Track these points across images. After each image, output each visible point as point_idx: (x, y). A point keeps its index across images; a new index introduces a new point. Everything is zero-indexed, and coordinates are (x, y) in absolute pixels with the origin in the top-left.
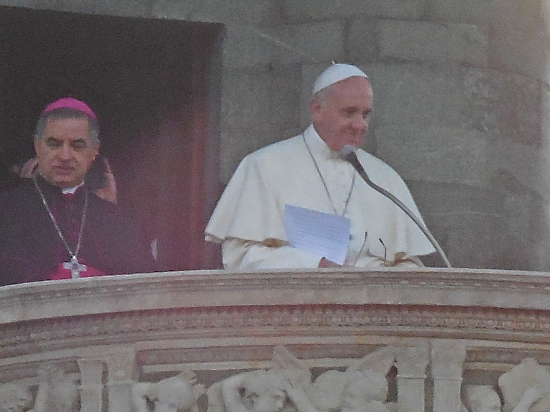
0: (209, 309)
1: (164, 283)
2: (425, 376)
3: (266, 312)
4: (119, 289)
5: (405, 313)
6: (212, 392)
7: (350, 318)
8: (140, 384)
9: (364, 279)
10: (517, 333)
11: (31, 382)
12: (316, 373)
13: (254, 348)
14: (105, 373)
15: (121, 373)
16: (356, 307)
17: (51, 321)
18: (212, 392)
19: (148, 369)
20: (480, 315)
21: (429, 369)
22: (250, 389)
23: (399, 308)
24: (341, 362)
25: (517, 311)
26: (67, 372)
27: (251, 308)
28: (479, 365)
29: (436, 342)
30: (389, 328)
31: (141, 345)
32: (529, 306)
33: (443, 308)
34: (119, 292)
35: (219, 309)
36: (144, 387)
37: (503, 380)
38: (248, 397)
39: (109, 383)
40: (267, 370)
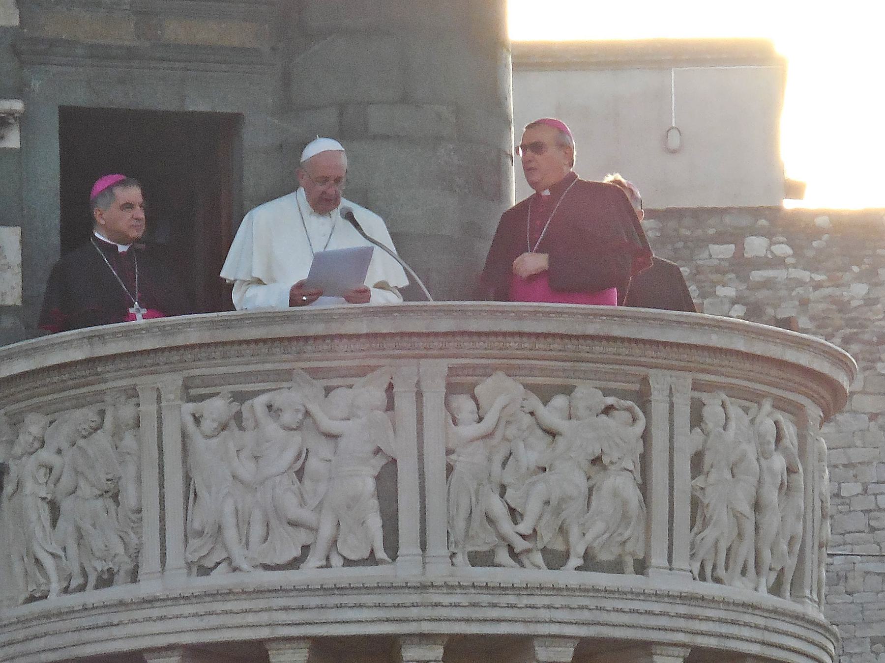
0: (240, 342)
1: (202, 322)
2: (416, 390)
9: (363, 313)
11: (100, 406)
12: (328, 390)
14: (159, 399)
15: (172, 396)
16: (358, 336)
17: (113, 358)
19: (193, 392)
20: (458, 338)
21: (418, 384)
22: (276, 405)
23: (392, 335)
24: (349, 381)
25: (487, 334)
26: (129, 397)
27: (273, 340)
28: (458, 379)
29: (423, 361)
30: (384, 353)
31: (186, 373)
32: (497, 329)
33: (428, 335)
34: (167, 330)
35: (248, 342)
36: (191, 407)
37: (478, 390)
40: (289, 388)
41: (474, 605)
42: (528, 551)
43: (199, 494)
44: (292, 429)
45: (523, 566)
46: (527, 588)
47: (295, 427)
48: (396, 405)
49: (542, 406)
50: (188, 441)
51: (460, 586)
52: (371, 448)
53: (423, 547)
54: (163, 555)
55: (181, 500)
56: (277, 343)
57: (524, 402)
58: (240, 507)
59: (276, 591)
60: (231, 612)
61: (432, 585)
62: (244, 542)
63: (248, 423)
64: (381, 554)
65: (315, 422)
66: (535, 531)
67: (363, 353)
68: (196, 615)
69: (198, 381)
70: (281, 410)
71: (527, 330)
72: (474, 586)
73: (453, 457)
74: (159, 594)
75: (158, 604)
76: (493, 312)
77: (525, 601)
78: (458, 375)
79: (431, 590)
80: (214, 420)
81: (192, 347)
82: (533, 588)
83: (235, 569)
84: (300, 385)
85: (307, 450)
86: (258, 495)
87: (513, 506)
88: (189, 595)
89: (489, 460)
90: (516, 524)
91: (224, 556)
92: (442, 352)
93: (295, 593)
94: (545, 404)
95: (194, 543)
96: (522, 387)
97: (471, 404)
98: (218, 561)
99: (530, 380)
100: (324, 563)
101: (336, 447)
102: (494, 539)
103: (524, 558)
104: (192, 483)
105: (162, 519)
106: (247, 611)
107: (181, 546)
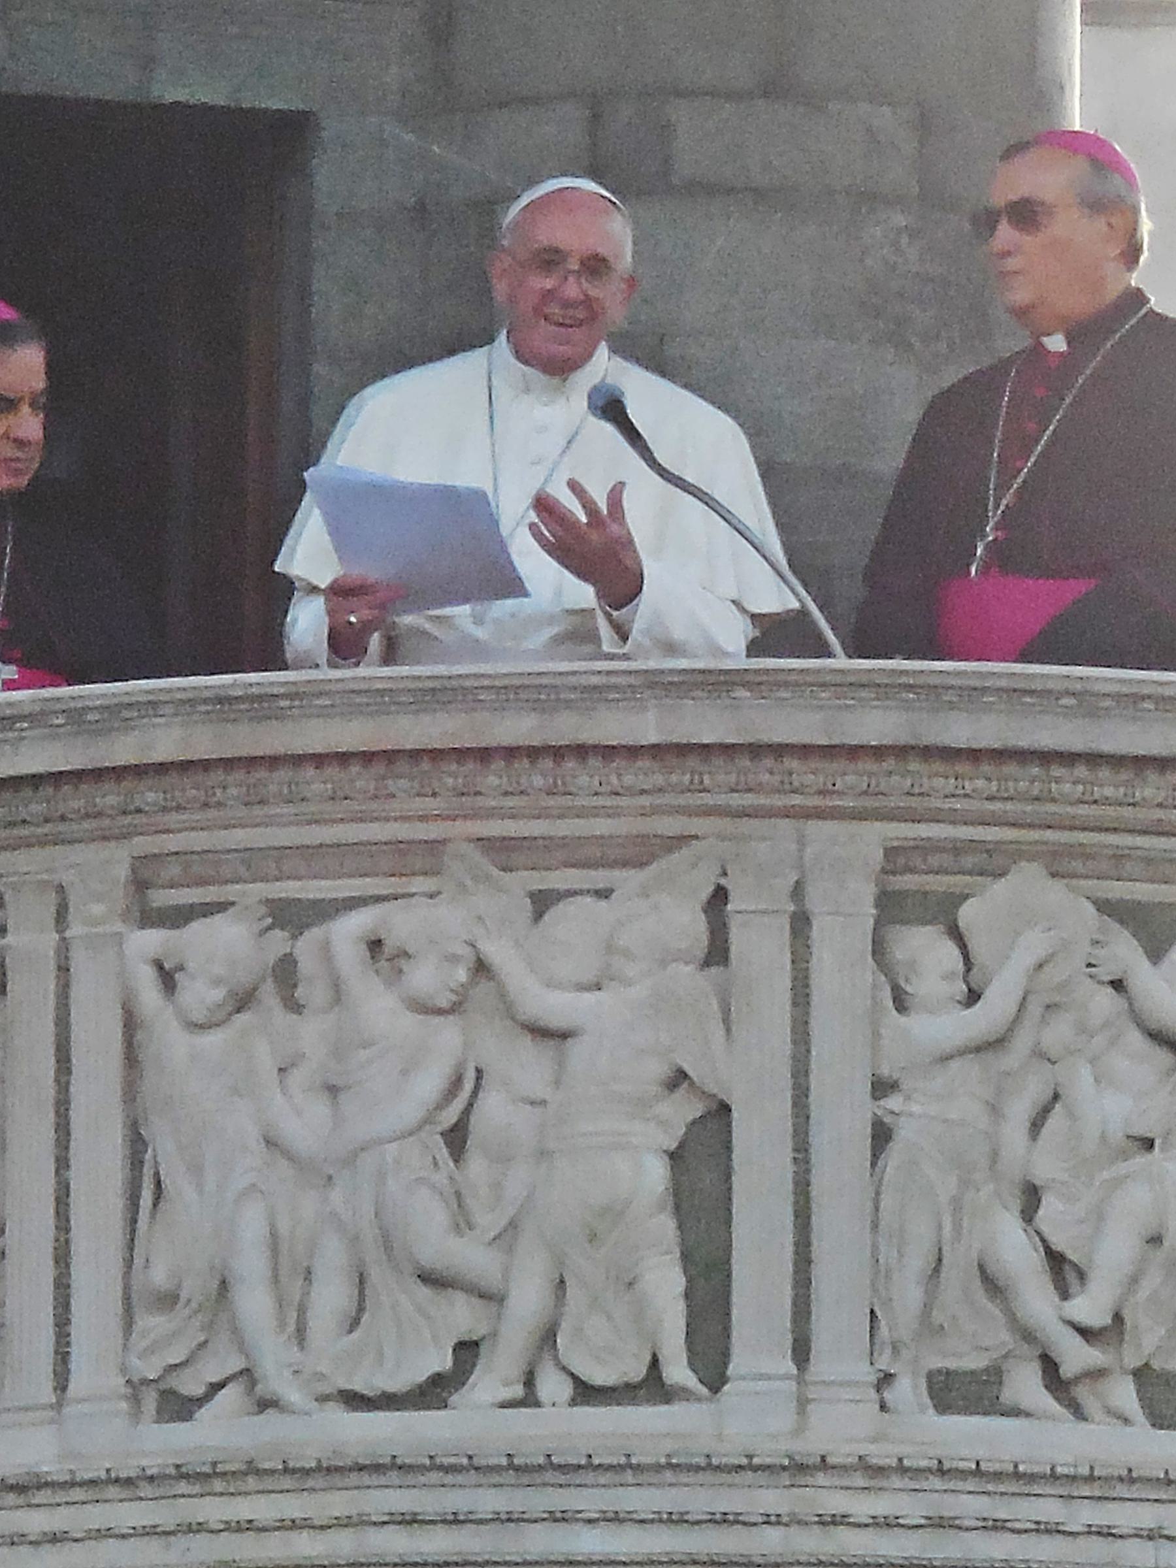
0: (298, 760)
3: (426, 765)
4: (90, 717)
5: (745, 762)
6: (305, 948)
7: (619, 775)
8: (139, 933)
9: (652, 686)
10: (997, 806)
12: (542, 902)
13: (400, 847)
15: (97, 909)
16: (633, 752)
18: (305, 948)
20: (914, 766)
21: (798, 891)
23: (728, 750)
24: (600, 878)
25: (1001, 755)
27: (390, 756)
29: (813, 827)
30: (707, 799)
31: (143, 844)
32: (1024, 743)
33: (830, 751)
35: (319, 760)
36: (151, 940)
37: (967, 914)
38: (388, 960)
39: (68, 934)
41: (939, 1523)
42: (1097, 1374)
43: (166, 1181)
44: (440, 1012)
45: (1078, 1412)
46: (1091, 1478)
47: (444, 1004)
48: (733, 949)
49: (1146, 964)
50: (139, 1036)
51: (902, 1469)
52: (658, 1069)
53: (801, 1352)
54: (62, 1357)
55: (117, 1203)
56: (402, 766)
57: (1101, 952)
58: (283, 1227)
59: (377, 1468)
60: (248, 1526)
61: (824, 1464)
62: (291, 1328)
63: (313, 992)
64: (678, 1372)
65: (502, 995)
66: (1118, 1318)
67: (645, 801)
68: (151, 1532)
69: (174, 870)
70: (406, 955)
71: (1107, 747)
72: (942, 1471)
73: (893, 1102)
74: (51, 1468)
75: (41, 1497)
76: (1015, 693)
77: (1088, 1514)
78: (912, 870)
79: (821, 1478)
80: (217, 982)
81: (162, 768)
82: (1107, 1479)
83: (265, 1404)
84: (462, 887)
85: (479, 1071)
86: (336, 1196)
87: (1059, 1243)
88: (133, 1474)
89: (995, 1110)
90: (1065, 1295)
91: (235, 1364)
92: (870, 803)
93: (434, 1477)
94: (1155, 955)
95: (151, 1323)
96: (1090, 909)
97: (949, 953)
98: (215, 1379)
99: (1116, 890)
100: (518, 1391)
101: (561, 1064)
102: (1005, 1337)
103: (1082, 1392)
104: (148, 1156)
105: (62, 1257)
106: (295, 1525)
107: (115, 1324)
